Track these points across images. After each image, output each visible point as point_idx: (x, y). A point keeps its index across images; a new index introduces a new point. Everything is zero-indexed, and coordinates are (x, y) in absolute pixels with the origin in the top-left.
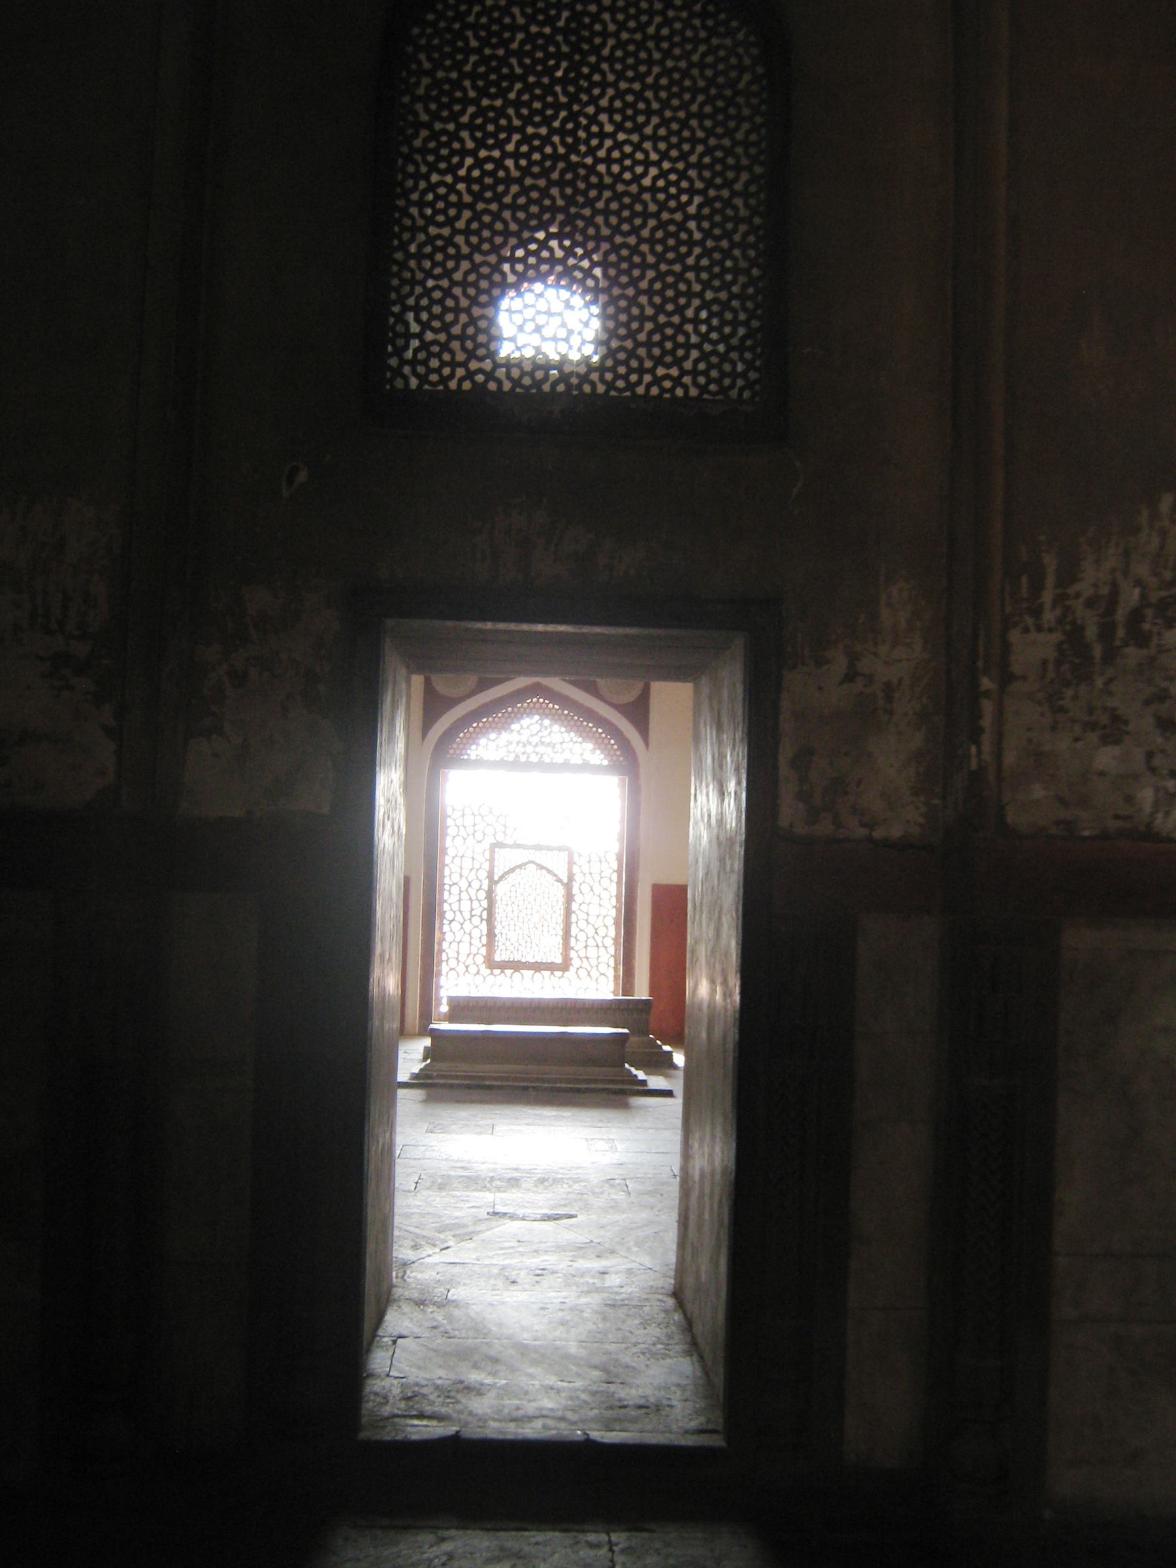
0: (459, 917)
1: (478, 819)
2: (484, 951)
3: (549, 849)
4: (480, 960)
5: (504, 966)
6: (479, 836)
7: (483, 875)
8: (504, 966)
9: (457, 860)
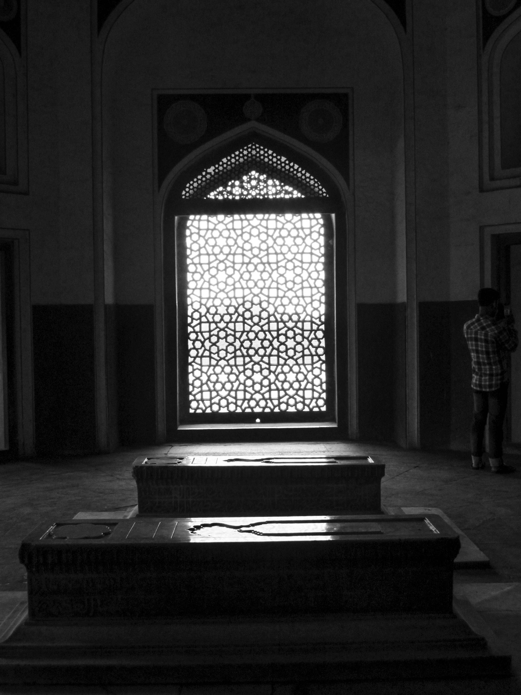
0: (200, 337)
1: (212, 258)
9: (197, 292)
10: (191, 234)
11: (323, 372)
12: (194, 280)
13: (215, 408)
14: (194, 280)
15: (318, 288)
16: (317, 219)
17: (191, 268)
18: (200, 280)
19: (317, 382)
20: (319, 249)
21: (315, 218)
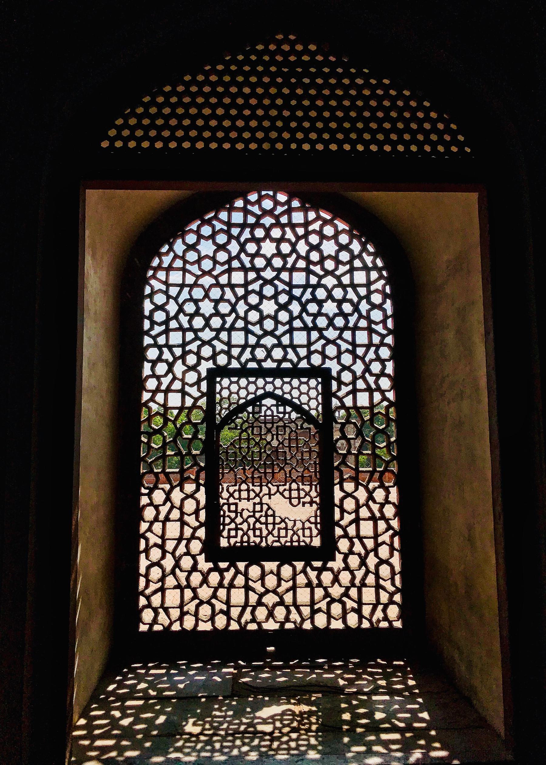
2: (201, 533)
3: (295, 372)
4: (196, 546)
5: (233, 555)
6: (191, 360)
7: (197, 416)
8: (233, 555)
9: (160, 398)
10: (153, 293)
11: (395, 552)
12: (153, 375)
13: (189, 623)
14: (154, 376)
15: (382, 392)
16: (379, 270)
17: (152, 354)
18: (166, 375)
19: (385, 570)
20: (384, 322)
21: (375, 267)
